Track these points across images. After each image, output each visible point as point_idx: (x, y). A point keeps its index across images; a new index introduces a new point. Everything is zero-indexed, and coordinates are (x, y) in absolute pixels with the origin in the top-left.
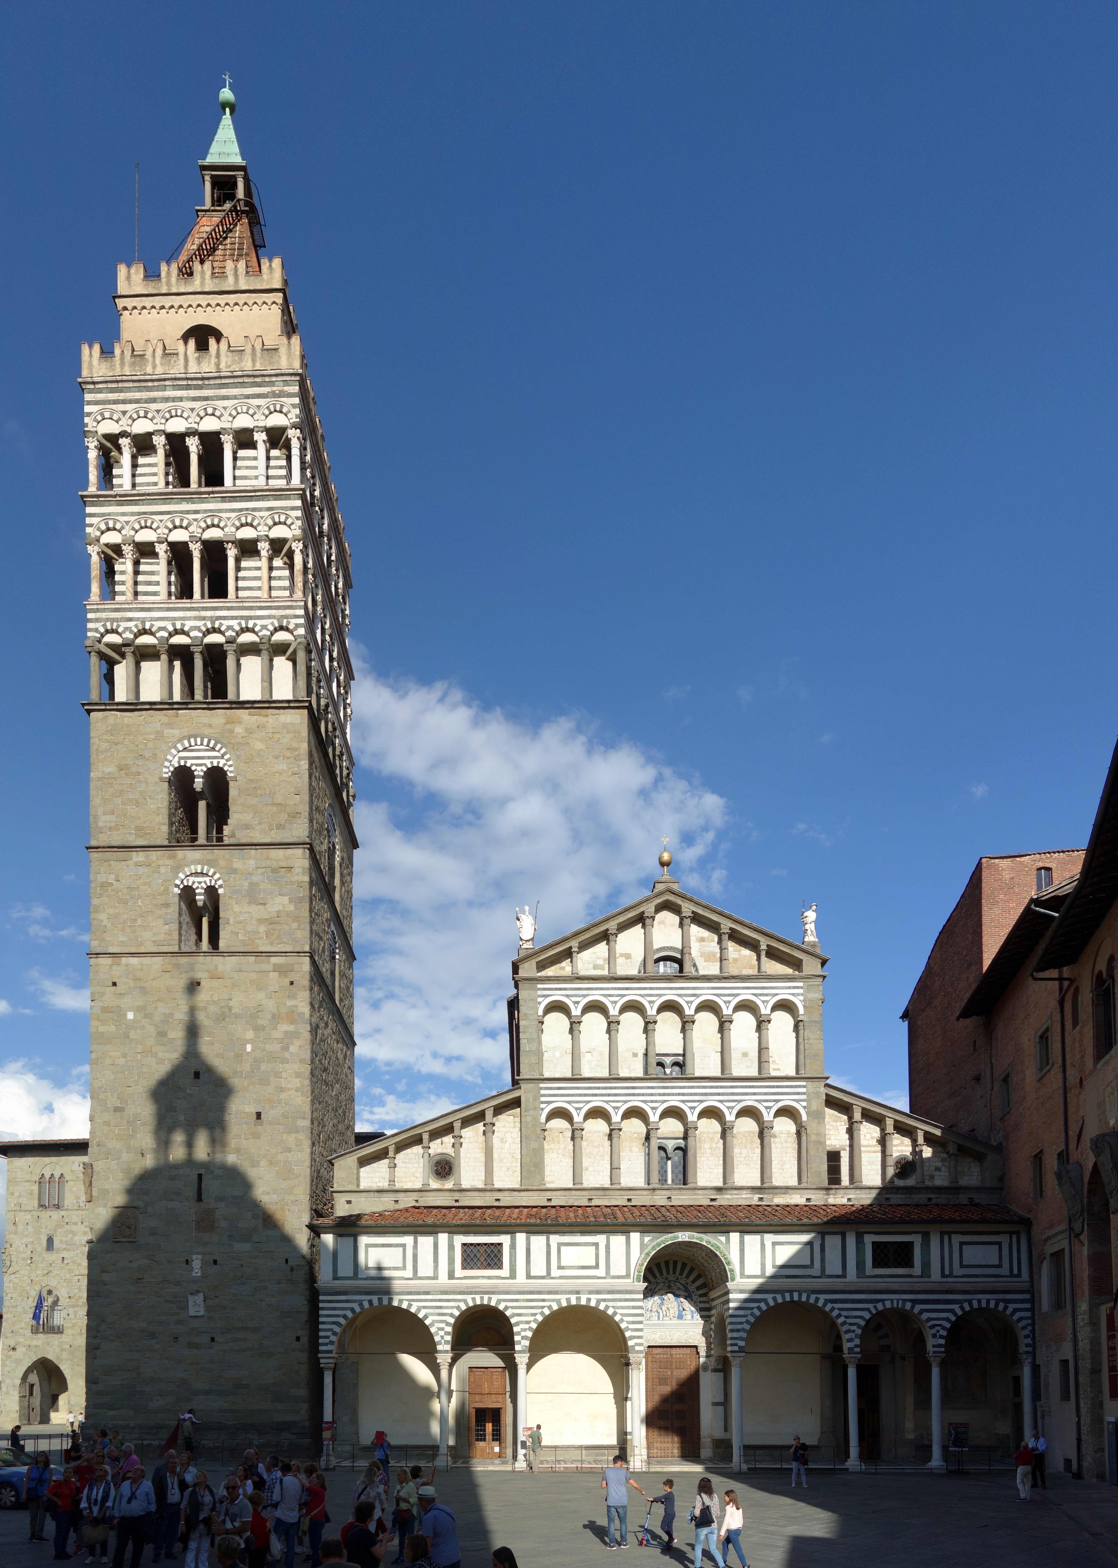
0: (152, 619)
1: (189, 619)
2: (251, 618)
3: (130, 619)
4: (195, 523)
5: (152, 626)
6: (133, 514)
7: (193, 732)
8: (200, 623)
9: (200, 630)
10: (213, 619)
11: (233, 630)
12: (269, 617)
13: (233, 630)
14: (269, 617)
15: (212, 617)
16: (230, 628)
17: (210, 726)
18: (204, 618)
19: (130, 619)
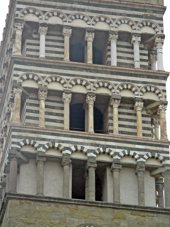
0: (59, 141)
1: (87, 144)
2: (132, 149)
3: (44, 140)
4: (92, 84)
5: (60, 145)
6: (47, 73)
7: (88, 223)
8: (93, 148)
9: (95, 153)
10: (105, 147)
11: (119, 156)
12: (145, 150)
13: (119, 156)
14: (145, 150)
15: (104, 145)
16: (116, 154)
17: (101, 218)
18: (98, 145)
19: (44, 140)
